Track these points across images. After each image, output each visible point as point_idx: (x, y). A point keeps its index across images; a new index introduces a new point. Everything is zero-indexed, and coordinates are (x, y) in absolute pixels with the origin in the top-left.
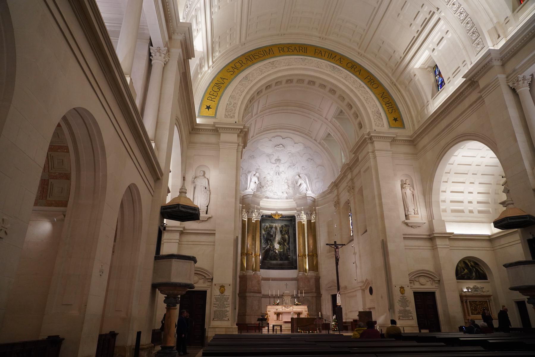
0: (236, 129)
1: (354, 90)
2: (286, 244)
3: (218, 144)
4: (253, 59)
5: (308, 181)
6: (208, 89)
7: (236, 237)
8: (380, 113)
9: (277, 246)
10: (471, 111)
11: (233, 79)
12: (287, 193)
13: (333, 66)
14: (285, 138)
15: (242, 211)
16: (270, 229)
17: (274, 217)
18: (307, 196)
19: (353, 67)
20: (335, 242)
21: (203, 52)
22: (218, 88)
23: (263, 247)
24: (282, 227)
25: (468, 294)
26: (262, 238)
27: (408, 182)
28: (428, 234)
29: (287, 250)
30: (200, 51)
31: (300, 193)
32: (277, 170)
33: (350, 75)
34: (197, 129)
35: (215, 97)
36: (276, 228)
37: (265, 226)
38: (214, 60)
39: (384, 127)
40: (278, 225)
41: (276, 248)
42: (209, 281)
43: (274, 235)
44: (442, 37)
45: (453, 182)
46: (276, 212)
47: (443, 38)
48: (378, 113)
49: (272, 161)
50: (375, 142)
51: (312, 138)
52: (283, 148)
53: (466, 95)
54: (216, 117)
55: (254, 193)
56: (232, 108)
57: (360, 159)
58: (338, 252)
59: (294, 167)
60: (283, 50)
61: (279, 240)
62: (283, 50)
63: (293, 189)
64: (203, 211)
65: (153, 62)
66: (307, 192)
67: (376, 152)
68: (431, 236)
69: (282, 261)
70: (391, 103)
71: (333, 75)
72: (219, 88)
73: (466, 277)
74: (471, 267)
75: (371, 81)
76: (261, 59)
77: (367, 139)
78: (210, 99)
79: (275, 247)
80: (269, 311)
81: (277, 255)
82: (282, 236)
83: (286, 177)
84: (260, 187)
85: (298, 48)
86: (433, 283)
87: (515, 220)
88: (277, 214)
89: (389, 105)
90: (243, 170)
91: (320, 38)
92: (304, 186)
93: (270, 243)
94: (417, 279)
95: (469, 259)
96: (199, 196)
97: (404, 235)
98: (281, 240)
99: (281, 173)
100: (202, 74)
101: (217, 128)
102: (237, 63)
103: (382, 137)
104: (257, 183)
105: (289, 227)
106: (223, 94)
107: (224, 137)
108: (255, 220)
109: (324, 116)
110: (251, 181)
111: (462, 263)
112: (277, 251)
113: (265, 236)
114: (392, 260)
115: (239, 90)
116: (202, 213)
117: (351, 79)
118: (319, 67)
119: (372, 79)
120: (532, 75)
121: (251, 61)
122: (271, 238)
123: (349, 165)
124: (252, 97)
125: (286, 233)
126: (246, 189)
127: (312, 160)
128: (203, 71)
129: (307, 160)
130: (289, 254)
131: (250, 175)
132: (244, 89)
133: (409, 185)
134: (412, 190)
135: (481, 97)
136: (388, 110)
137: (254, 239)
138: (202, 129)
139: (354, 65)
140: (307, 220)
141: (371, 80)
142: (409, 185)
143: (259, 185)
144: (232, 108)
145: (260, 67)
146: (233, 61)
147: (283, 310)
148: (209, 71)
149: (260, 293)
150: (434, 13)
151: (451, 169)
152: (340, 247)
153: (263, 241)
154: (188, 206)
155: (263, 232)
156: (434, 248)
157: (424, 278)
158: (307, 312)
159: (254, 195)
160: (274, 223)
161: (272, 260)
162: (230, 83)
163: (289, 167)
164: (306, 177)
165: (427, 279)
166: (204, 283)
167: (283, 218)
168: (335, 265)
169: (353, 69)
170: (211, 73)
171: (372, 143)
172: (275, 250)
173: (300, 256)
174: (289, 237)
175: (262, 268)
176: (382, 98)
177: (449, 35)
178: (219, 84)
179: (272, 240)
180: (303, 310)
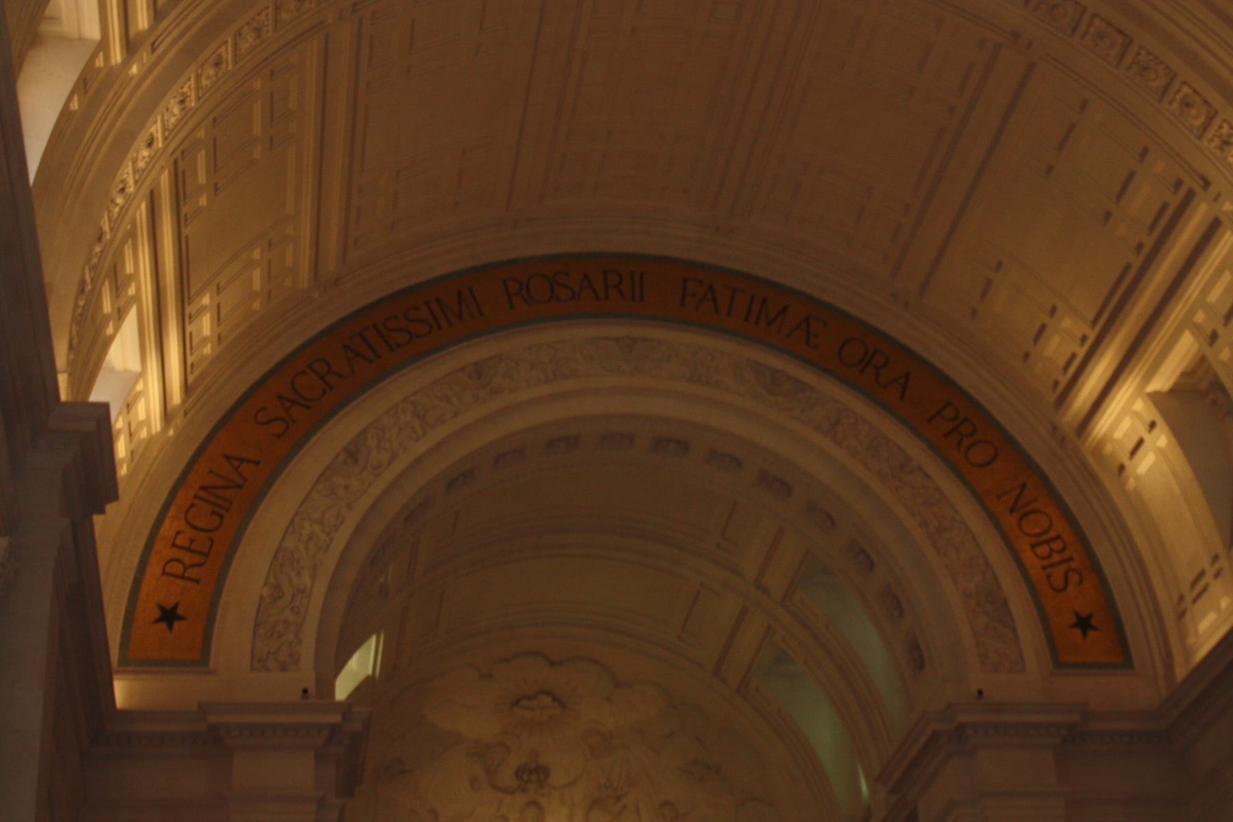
6: (167, 521)
8: (1005, 602)
30: (125, 371)
35: (197, 559)
70: (1059, 537)
89: (1052, 550)
102: (303, 373)
121: (371, 362)
145: (415, 394)
148: (171, 432)
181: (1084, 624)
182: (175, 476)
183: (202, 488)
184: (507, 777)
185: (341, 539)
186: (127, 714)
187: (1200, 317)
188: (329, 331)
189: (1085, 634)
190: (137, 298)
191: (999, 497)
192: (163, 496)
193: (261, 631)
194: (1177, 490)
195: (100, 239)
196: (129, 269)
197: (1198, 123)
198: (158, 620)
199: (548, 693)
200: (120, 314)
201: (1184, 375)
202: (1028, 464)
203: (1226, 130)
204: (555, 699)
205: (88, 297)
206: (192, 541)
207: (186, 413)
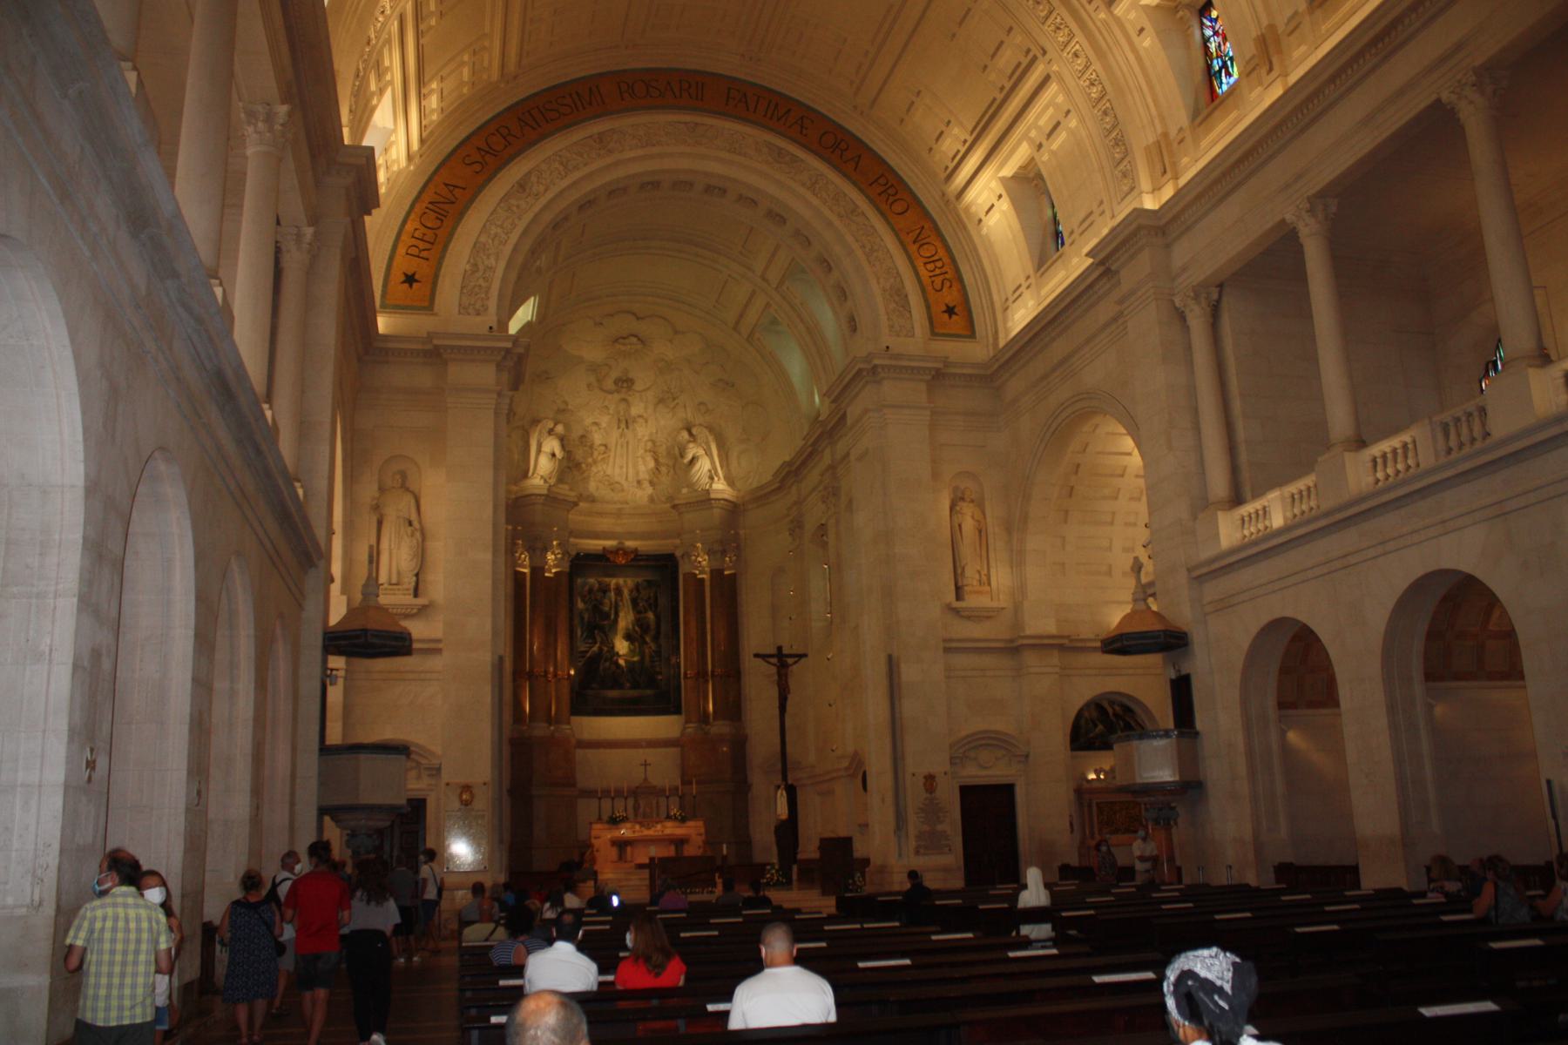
0: (493, 349)
1: (837, 222)
2: (648, 639)
6: (409, 222)
8: (906, 296)
9: (622, 646)
11: (480, 189)
12: (652, 483)
14: (642, 318)
15: (514, 544)
16: (599, 595)
17: (612, 559)
18: (713, 496)
20: (780, 649)
23: (582, 649)
24: (637, 588)
25: (1096, 785)
26: (577, 621)
31: (690, 485)
35: (427, 246)
36: (618, 591)
39: (913, 336)
40: (625, 581)
41: (618, 653)
42: (429, 775)
43: (613, 612)
46: (620, 543)
47: (1058, 124)
48: (899, 295)
54: (432, 310)
55: (549, 490)
56: (481, 282)
57: (849, 422)
61: (627, 629)
64: (408, 590)
66: (711, 486)
70: (940, 259)
72: (439, 216)
75: (890, 191)
77: (865, 373)
78: (414, 251)
79: (616, 650)
80: (596, 838)
81: (623, 671)
82: (638, 616)
83: (651, 434)
84: (569, 468)
88: (621, 549)
89: (936, 267)
91: (743, 56)
92: (704, 465)
96: (393, 546)
97: (945, 641)
98: (634, 628)
101: (437, 347)
102: (493, 134)
104: (559, 454)
107: (461, 373)
108: (554, 571)
110: (539, 451)
112: (622, 662)
113: (586, 616)
114: (909, 707)
116: (404, 594)
119: (892, 185)
120: (1221, 286)
121: (534, 129)
122: (605, 623)
125: (650, 605)
130: (658, 669)
131: (537, 434)
133: (971, 505)
134: (976, 518)
135: (1120, 314)
137: (550, 630)
139: (842, 140)
140: (712, 571)
141: (888, 189)
144: (481, 282)
145: (561, 151)
146: (479, 128)
147: (636, 835)
148: (412, 168)
149: (574, 785)
152: (790, 661)
153: (579, 633)
155: (580, 605)
158: (703, 837)
159: (551, 498)
164: (711, 438)
166: (419, 777)
167: (638, 561)
168: (777, 712)
172: (615, 658)
174: (658, 617)
176: (917, 245)
177: (1073, 123)
178: (441, 206)
180: (693, 830)
181: (950, 311)
183: (430, 203)
184: (609, 384)
185: (514, 237)
186: (386, 337)
187: (1033, 134)
188: (509, 109)
189: (950, 317)
190: (391, 83)
191: (908, 233)
192: (407, 207)
193: (465, 291)
194: (1011, 237)
195: (368, 43)
196: (387, 63)
197: (1043, 14)
198: (404, 282)
199: (635, 336)
200: (381, 92)
201: (1021, 168)
202: (926, 214)
203: (1058, 20)
204: (639, 339)
205: (361, 79)
206: (424, 234)
207: (421, 156)
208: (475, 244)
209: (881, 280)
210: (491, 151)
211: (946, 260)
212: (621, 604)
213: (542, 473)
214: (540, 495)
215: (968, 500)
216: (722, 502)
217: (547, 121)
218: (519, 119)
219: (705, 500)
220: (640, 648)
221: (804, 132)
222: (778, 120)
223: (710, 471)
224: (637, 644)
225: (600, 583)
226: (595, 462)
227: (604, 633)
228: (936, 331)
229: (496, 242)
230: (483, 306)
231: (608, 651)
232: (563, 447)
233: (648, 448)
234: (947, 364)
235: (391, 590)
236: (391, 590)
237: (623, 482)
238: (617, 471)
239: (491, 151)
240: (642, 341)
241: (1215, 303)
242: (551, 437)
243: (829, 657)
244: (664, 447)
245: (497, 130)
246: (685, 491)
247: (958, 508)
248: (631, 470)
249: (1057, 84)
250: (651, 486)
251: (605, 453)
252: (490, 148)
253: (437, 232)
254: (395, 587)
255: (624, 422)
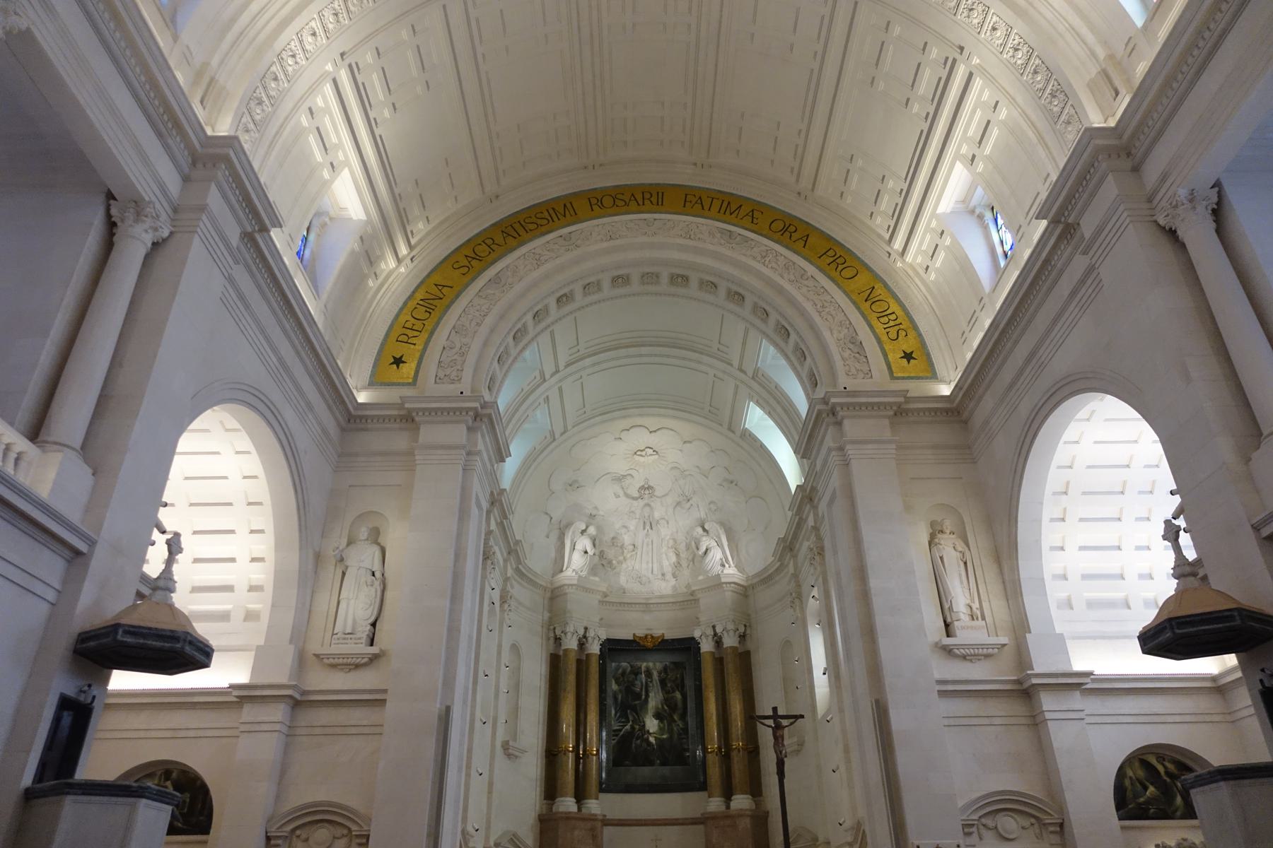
0: (461, 410)
1: (787, 286)
2: (676, 718)
3: (410, 453)
4: (521, 231)
5: (728, 540)
7: (444, 708)
8: (861, 342)
9: (652, 724)
10: (1077, 310)
11: (467, 285)
12: (674, 576)
13: (730, 231)
14: (655, 431)
16: (633, 676)
17: (642, 643)
18: (723, 580)
19: (786, 230)
20: (775, 709)
21: (369, 221)
22: (426, 311)
24: (665, 669)
26: (610, 701)
27: (948, 525)
28: (1015, 678)
29: (679, 734)
30: (361, 220)
32: (646, 515)
33: (776, 252)
34: (361, 417)
35: (416, 333)
36: (649, 673)
37: (618, 668)
38: (413, 242)
40: (654, 664)
41: (648, 731)
42: (360, 844)
43: (644, 693)
44: (986, 122)
45: (1081, 520)
47: (989, 122)
48: (853, 343)
49: (629, 492)
50: (846, 422)
51: (721, 425)
52: (657, 456)
53: (1059, 265)
55: (578, 580)
58: (783, 740)
59: (689, 504)
60: (602, 203)
61: (657, 708)
62: (602, 203)
63: (692, 563)
64: (360, 639)
65: (115, 239)
66: (722, 572)
67: (848, 447)
68: (1026, 685)
69: (668, 767)
70: (893, 313)
71: (729, 253)
72: (428, 310)
73: (1152, 811)
74: (1165, 778)
75: (837, 261)
76: (543, 229)
77: (824, 415)
78: (404, 338)
79: (647, 728)
82: (666, 696)
84: (603, 565)
85: (639, 197)
86: (1041, 831)
87: (1195, 629)
89: (889, 320)
90: (552, 521)
91: (695, 164)
92: (716, 555)
93: (634, 716)
94: (989, 822)
95: (1160, 751)
99: (658, 522)
100: (381, 279)
101: (410, 411)
103: (867, 405)
105: (685, 668)
106: (437, 324)
107: (429, 434)
109: (736, 363)
111: (1137, 764)
112: (652, 739)
114: (903, 759)
115: (478, 311)
116: (356, 644)
117: (777, 260)
118: (692, 237)
119: (841, 256)
120: (1217, 184)
121: (515, 238)
122: (637, 702)
123: (806, 491)
124: (519, 326)
126: (562, 571)
127: (732, 482)
128: (383, 270)
129: (721, 485)
130: (686, 747)
132: (491, 306)
133: (952, 536)
134: (960, 549)
136: (887, 333)
138: (372, 417)
142: (954, 534)
143: (597, 558)
145: (534, 249)
146: (469, 241)
150: (955, 61)
151: (1068, 483)
152: (785, 722)
153: (613, 712)
154: (150, 629)
155: (614, 687)
156: (1036, 723)
157: (1012, 817)
159: (582, 586)
160: (644, 660)
161: (636, 763)
162: (457, 296)
163: (676, 506)
165: (1026, 822)
167: (665, 646)
169: (787, 234)
170: (408, 275)
171: (839, 424)
172: (646, 736)
173: (711, 752)
175: (605, 788)
176: (869, 303)
177: (1003, 113)
178: (431, 302)
179: (638, 708)
181: (908, 356)
182: (408, 294)
183: (421, 300)
190: (347, 163)
192: (400, 304)
199: (650, 448)
208: (454, 327)
209: (835, 332)
210: (478, 257)
211: (899, 312)
212: (651, 685)
213: (574, 568)
214: (572, 585)
215: (948, 532)
216: (732, 585)
217: (527, 232)
218: (502, 232)
219: (717, 584)
220: (668, 726)
221: (755, 221)
222: (731, 214)
223: (721, 559)
224: (665, 721)
225: (632, 666)
226: (625, 559)
227: (637, 714)
228: (895, 375)
229: (474, 323)
230: (458, 377)
231: (639, 730)
232: (594, 545)
233: (670, 546)
234: (908, 400)
235: (344, 639)
236: (344, 639)
237: (650, 575)
238: (644, 566)
239: (478, 257)
240: (657, 452)
241: (1215, 207)
242: (583, 537)
243: (828, 719)
244: (684, 544)
245: (483, 241)
246: (701, 578)
247: (936, 540)
248: (655, 566)
249: (981, 78)
250: (674, 578)
251: (633, 551)
252: (477, 255)
253: (424, 322)
254: (351, 636)
255: (648, 524)
